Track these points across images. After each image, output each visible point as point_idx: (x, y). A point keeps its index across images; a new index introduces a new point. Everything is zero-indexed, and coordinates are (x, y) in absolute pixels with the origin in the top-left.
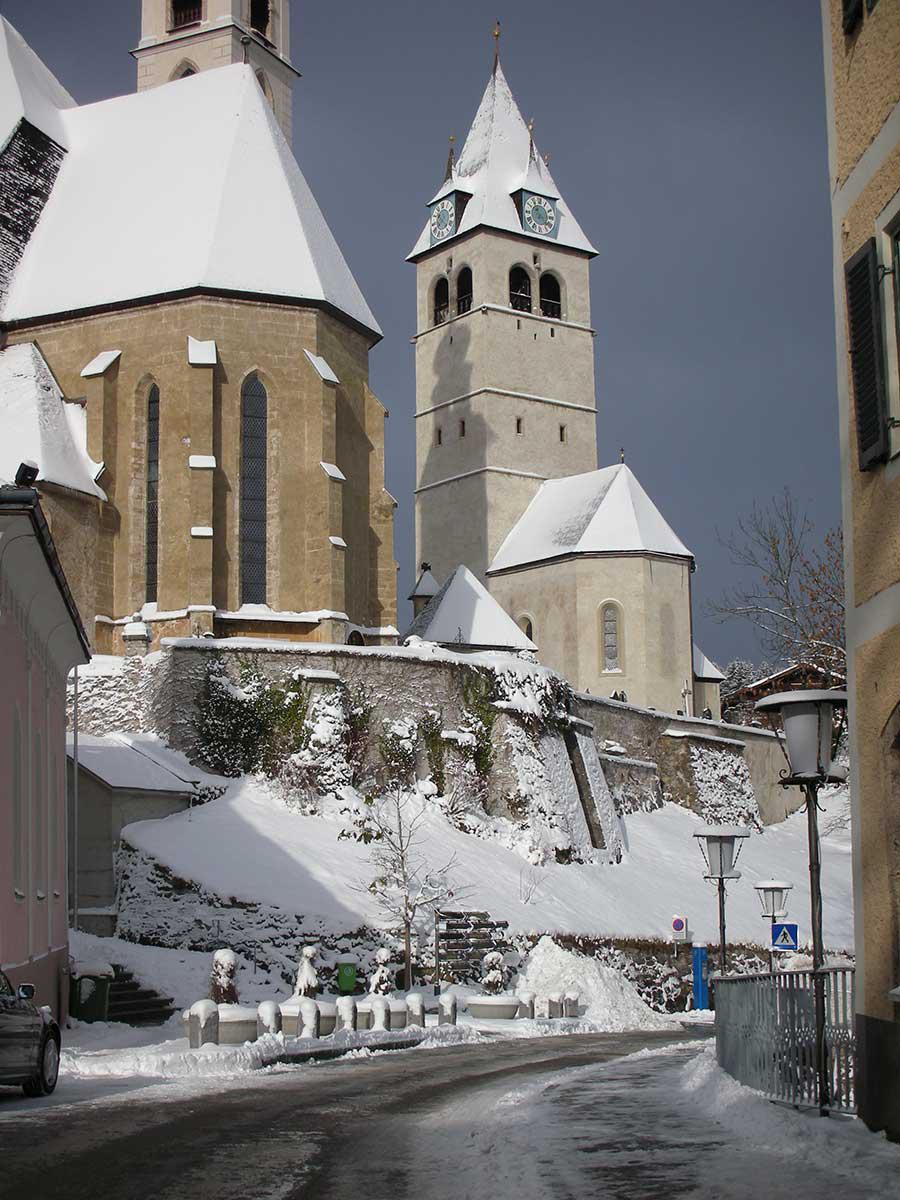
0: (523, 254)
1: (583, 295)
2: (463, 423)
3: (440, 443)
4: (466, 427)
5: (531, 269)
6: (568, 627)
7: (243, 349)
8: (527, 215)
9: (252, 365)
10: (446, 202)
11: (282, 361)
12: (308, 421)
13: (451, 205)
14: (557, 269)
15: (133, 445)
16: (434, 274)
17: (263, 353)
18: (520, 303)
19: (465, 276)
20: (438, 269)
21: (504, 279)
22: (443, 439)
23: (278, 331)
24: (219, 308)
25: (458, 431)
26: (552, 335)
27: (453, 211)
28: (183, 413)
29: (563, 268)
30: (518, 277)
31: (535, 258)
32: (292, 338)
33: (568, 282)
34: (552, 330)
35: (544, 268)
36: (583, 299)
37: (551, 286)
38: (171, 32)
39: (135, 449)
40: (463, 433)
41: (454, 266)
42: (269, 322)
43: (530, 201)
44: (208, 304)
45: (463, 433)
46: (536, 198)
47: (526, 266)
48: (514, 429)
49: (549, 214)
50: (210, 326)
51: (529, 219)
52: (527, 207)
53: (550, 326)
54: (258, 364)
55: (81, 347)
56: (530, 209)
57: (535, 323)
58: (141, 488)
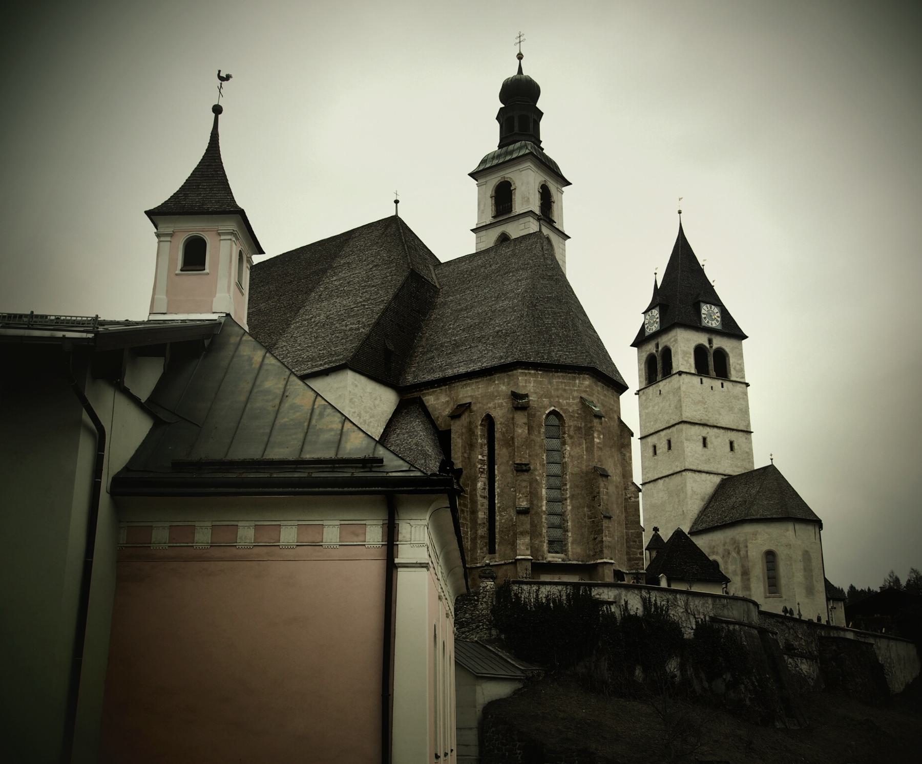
0: (702, 339)
4: (672, 445)
5: (707, 348)
6: (743, 566)
7: (545, 398)
9: (551, 407)
10: (653, 311)
11: (568, 404)
12: (585, 440)
13: (656, 312)
14: (724, 347)
15: (480, 457)
16: (648, 353)
17: (557, 399)
18: (702, 369)
19: (667, 353)
20: (650, 349)
21: (691, 354)
23: (565, 386)
24: (530, 373)
25: (666, 446)
26: (722, 387)
27: (658, 316)
28: (509, 437)
29: (726, 346)
31: (710, 341)
32: (575, 390)
33: (731, 355)
34: (722, 384)
35: (715, 346)
38: (494, 217)
39: (481, 460)
40: (670, 448)
41: (660, 348)
42: (560, 381)
43: (705, 307)
44: (523, 371)
45: (670, 448)
46: (708, 305)
47: (705, 346)
48: (701, 444)
50: (524, 384)
51: (705, 318)
54: (554, 406)
55: (447, 399)
56: (706, 312)
58: (485, 483)
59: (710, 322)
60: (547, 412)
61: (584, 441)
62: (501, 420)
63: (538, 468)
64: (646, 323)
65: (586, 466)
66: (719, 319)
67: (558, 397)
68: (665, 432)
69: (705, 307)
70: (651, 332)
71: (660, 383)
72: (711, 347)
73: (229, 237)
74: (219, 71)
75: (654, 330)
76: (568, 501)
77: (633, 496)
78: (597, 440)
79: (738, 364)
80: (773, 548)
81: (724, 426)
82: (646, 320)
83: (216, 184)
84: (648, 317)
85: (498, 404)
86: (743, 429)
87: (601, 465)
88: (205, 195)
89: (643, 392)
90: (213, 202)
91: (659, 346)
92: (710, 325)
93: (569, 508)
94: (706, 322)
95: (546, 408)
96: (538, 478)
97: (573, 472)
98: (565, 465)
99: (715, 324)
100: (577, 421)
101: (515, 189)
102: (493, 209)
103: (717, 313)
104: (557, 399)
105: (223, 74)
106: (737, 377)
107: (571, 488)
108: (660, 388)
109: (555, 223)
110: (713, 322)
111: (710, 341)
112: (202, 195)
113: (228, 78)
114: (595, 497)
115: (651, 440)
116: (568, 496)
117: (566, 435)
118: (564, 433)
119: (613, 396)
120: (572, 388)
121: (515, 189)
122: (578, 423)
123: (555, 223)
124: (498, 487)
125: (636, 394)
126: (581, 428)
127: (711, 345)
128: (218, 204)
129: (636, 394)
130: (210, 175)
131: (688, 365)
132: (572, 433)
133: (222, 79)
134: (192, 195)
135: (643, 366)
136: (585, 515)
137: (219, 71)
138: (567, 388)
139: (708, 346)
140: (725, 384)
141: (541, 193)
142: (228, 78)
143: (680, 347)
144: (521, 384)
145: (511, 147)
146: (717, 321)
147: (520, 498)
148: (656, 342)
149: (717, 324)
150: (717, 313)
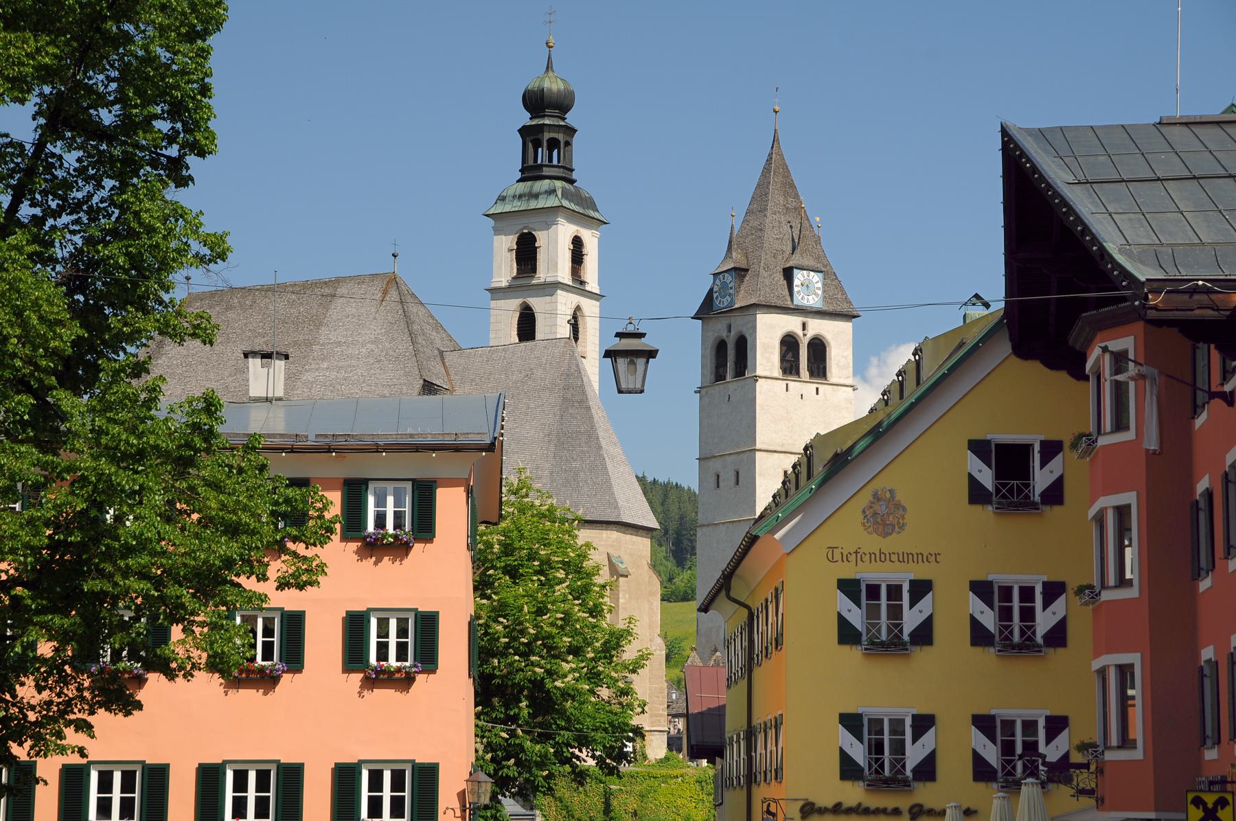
0: (791, 323)
1: (845, 354)
2: (738, 473)
3: (718, 487)
8: (796, 289)
10: (726, 275)
16: (716, 335)
18: (789, 367)
22: (721, 484)
25: (733, 479)
26: (817, 393)
30: (789, 344)
31: (804, 326)
34: (817, 389)
35: (811, 333)
36: (846, 358)
37: (818, 348)
40: (737, 483)
43: (799, 276)
45: (737, 483)
46: (805, 272)
47: (795, 334)
49: (816, 286)
51: (799, 292)
52: (796, 282)
53: (816, 385)
57: (803, 387)
59: (806, 297)
64: (715, 290)
66: (820, 292)
68: (732, 457)
69: (799, 276)
71: (730, 385)
72: (805, 335)
79: (843, 357)
82: (715, 286)
84: (718, 282)
89: (707, 392)
92: (805, 302)
94: (800, 298)
99: (813, 300)
103: (818, 282)
108: (730, 393)
110: (810, 298)
111: (804, 326)
115: (715, 465)
125: (696, 392)
127: (805, 332)
129: (696, 392)
131: (770, 364)
135: (708, 351)
139: (800, 332)
146: (816, 294)
149: (816, 299)
150: (818, 282)
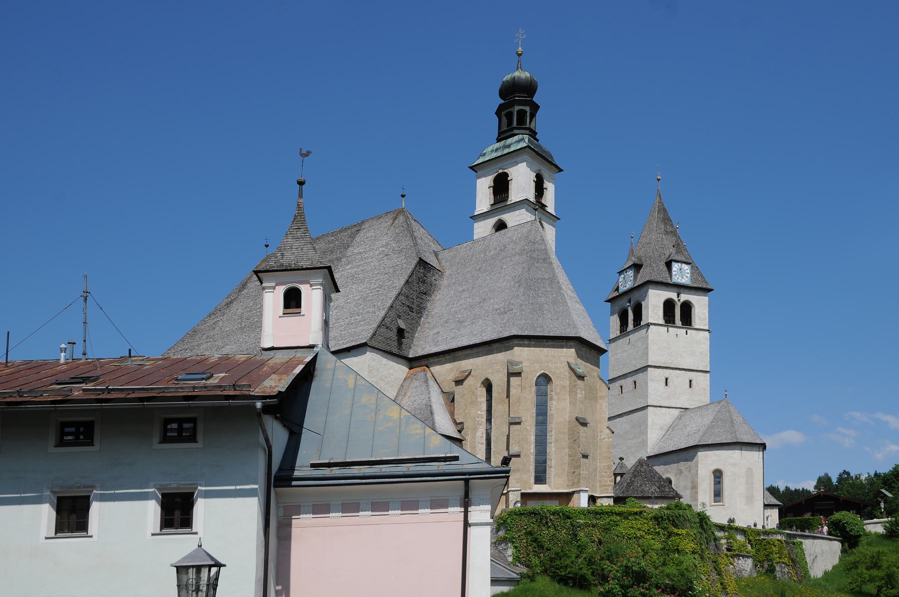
9: (541, 370)
17: (546, 364)
60: (538, 375)
61: (568, 397)
62: (498, 382)
63: (528, 420)
65: (569, 417)
67: (547, 362)
70: (625, 289)
73: (319, 287)
74: (301, 149)
75: (627, 287)
76: (553, 444)
77: (607, 437)
78: (579, 396)
80: (721, 467)
81: (685, 368)
83: (305, 244)
85: (496, 369)
86: (702, 370)
87: (581, 415)
88: (298, 254)
90: (305, 259)
91: (632, 300)
93: (553, 449)
95: (537, 372)
96: (528, 427)
97: (558, 422)
98: (551, 416)
100: (563, 381)
101: (512, 179)
102: (491, 198)
104: (546, 364)
105: (304, 152)
106: (700, 325)
107: (555, 434)
109: (547, 207)
112: (296, 254)
113: (308, 154)
114: (575, 440)
116: (552, 440)
117: (553, 393)
118: (552, 391)
119: (594, 358)
120: (560, 354)
121: (512, 179)
122: (564, 383)
123: (547, 207)
124: (494, 436)
126: (566, 386)
128: (309, 261)
130: (300, 237)
132: (558, 390)
133: (303, 155)
134: (287, 254)
136: (566, 454)
137: (301, 149)
138: (555, 354)
140: (689, 331)
141: (535, 182)
142: (308, 154)
143: (651, 302)
144: (516, 353)
145: (509, 141)
147: (513, 444)
148: (629, 298)
